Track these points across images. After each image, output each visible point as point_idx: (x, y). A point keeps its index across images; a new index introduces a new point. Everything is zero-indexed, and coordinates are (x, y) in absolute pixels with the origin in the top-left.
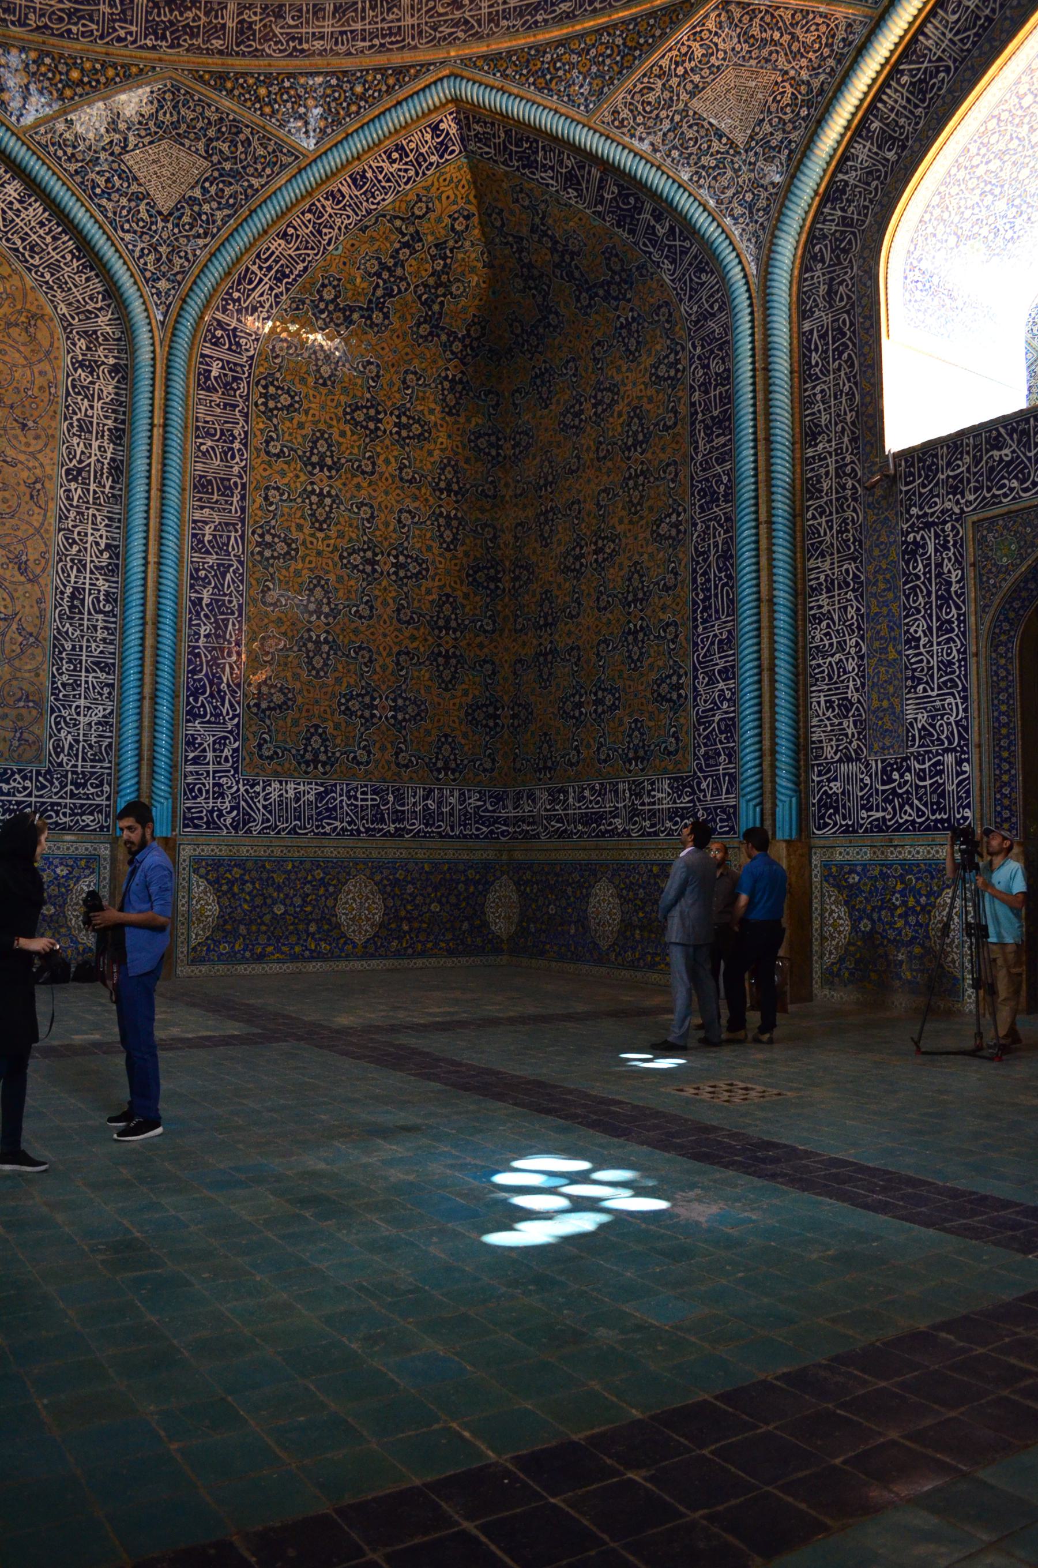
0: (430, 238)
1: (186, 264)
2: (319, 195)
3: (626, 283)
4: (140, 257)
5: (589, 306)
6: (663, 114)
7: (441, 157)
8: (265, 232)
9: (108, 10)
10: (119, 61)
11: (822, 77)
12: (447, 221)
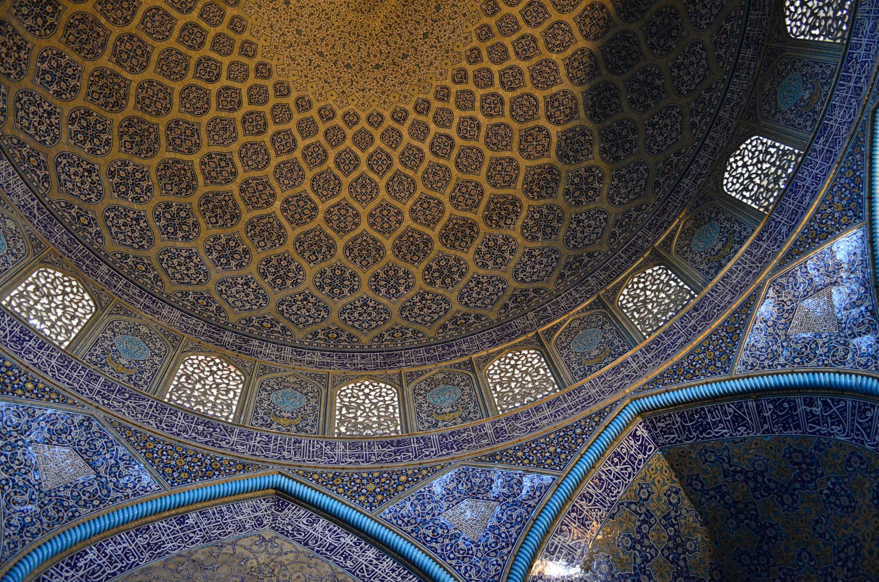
0: (658, 513)
1: (499, 568)
2: (576, 498)
3: (812, 465)
4: (466, 573)
5: (794, 501)
6: (775, 347)
7: (645, 454)
8: (548, 532)
9: (416, 445)
10: (428, 465)
11: (860, 268)
12: (664, 498)
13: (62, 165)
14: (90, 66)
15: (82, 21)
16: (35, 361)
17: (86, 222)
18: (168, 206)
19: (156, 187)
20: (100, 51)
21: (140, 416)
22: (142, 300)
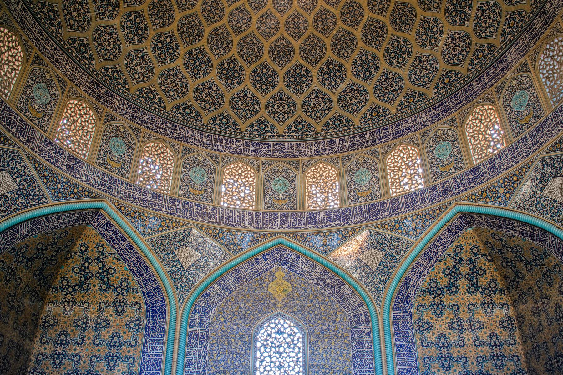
13: (415, 80)
14: (361, 44)
15: (335, 46)
16: (505, 167)
17: (448, 79)
18: (447, 10)
19: (434, 15)
20: (352, 36)
21: (553, 132)
22: (498, 70)
